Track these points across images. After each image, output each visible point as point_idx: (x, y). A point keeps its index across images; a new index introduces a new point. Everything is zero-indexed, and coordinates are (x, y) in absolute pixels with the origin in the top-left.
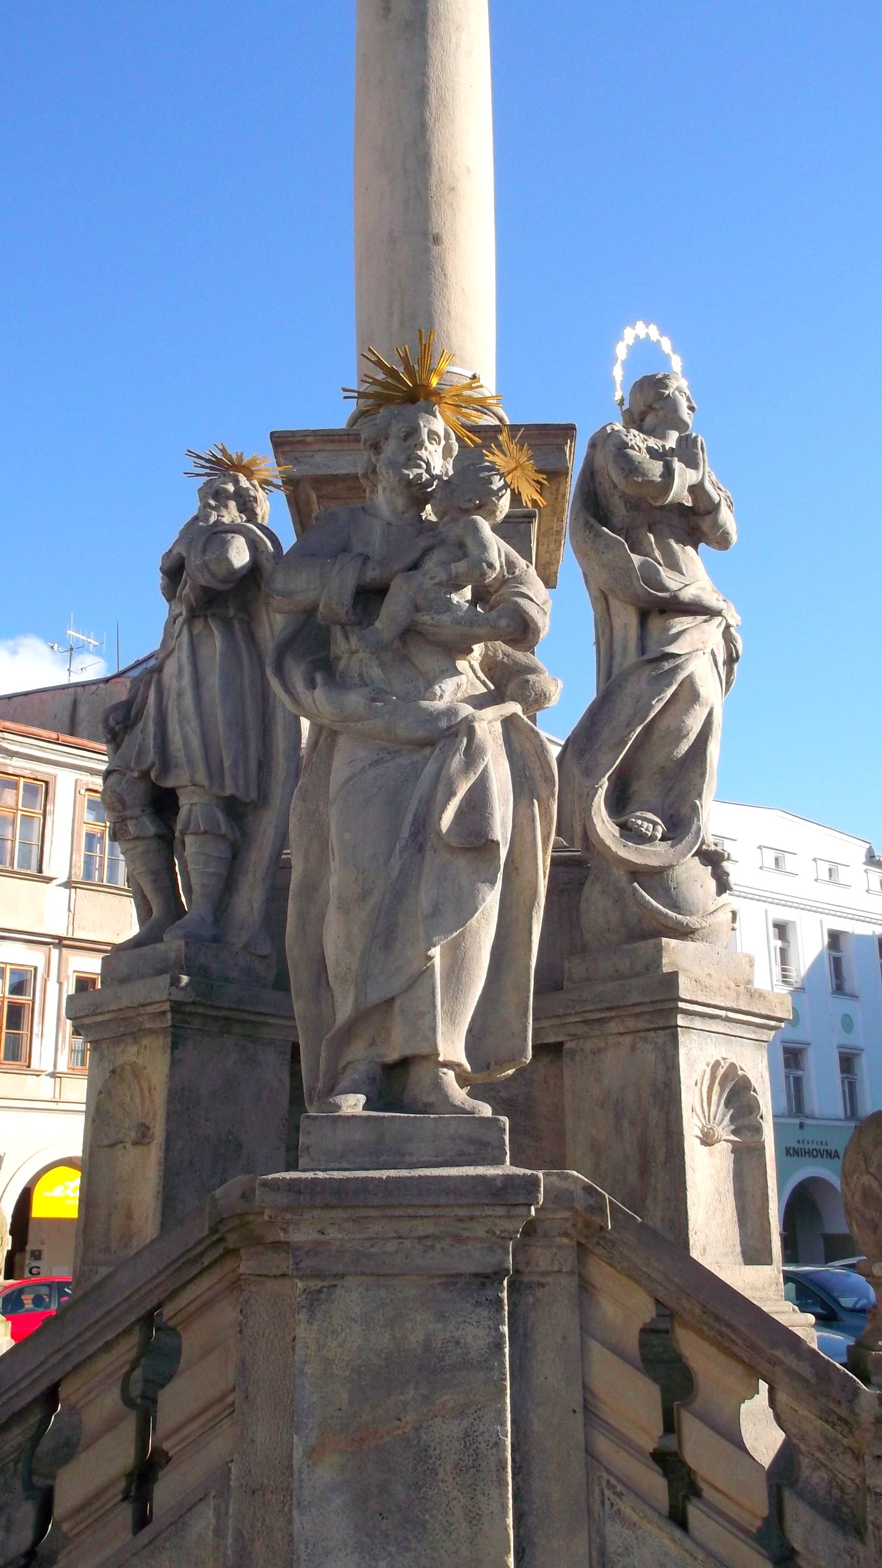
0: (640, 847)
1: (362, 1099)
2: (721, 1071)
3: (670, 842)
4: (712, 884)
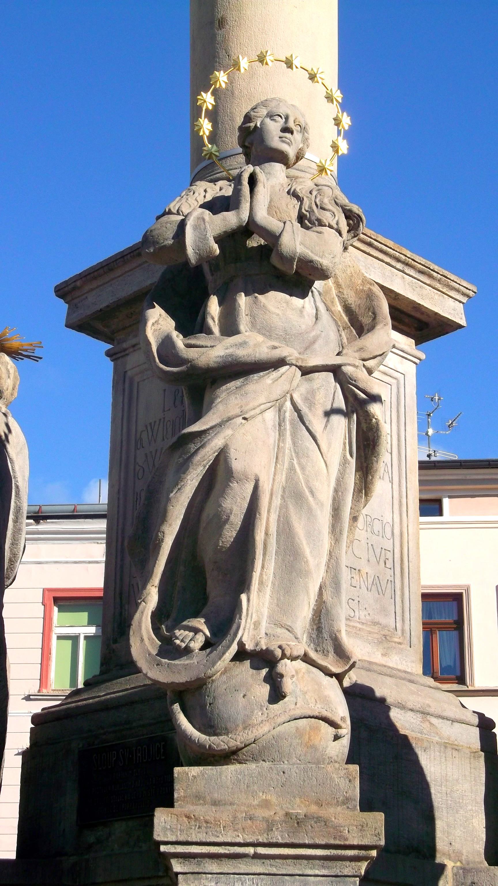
0: (177, 662)
3: (208, 650)
4: (266, 689)
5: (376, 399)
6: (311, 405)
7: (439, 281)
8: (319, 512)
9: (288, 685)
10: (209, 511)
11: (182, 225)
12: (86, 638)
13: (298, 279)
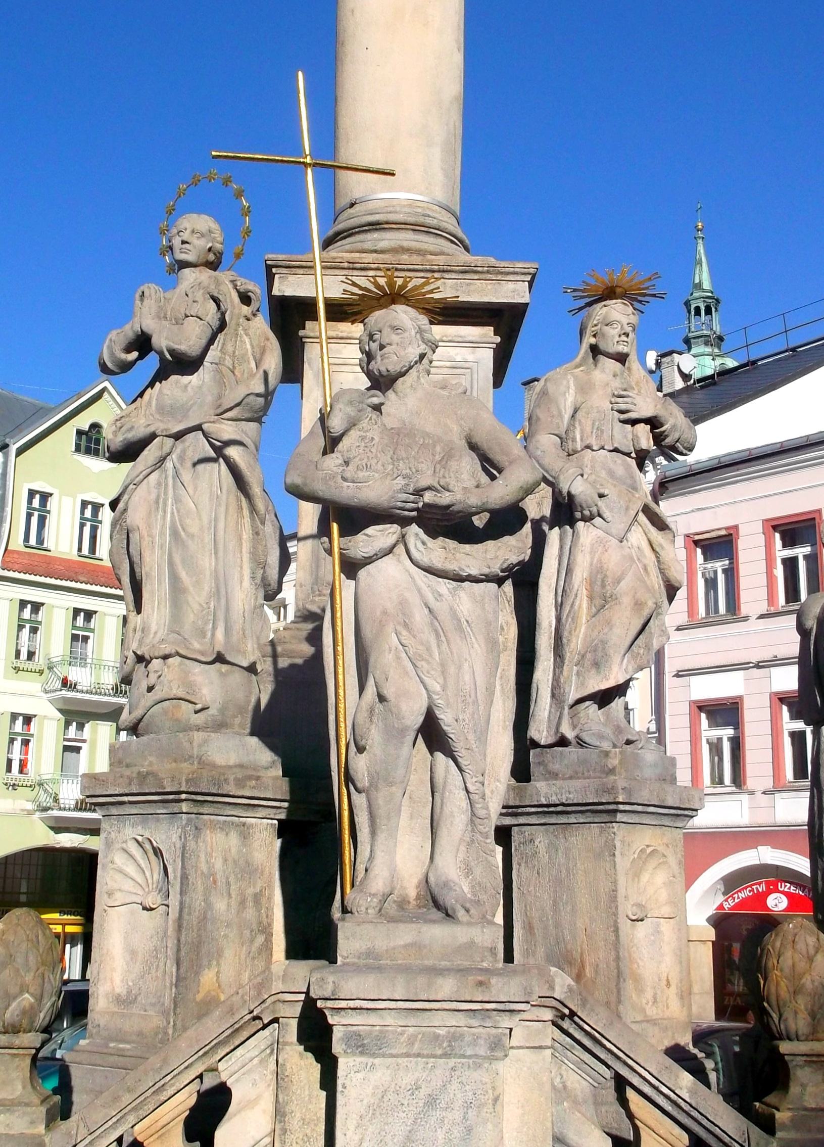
7: (488, 272)
8: (190, 542)
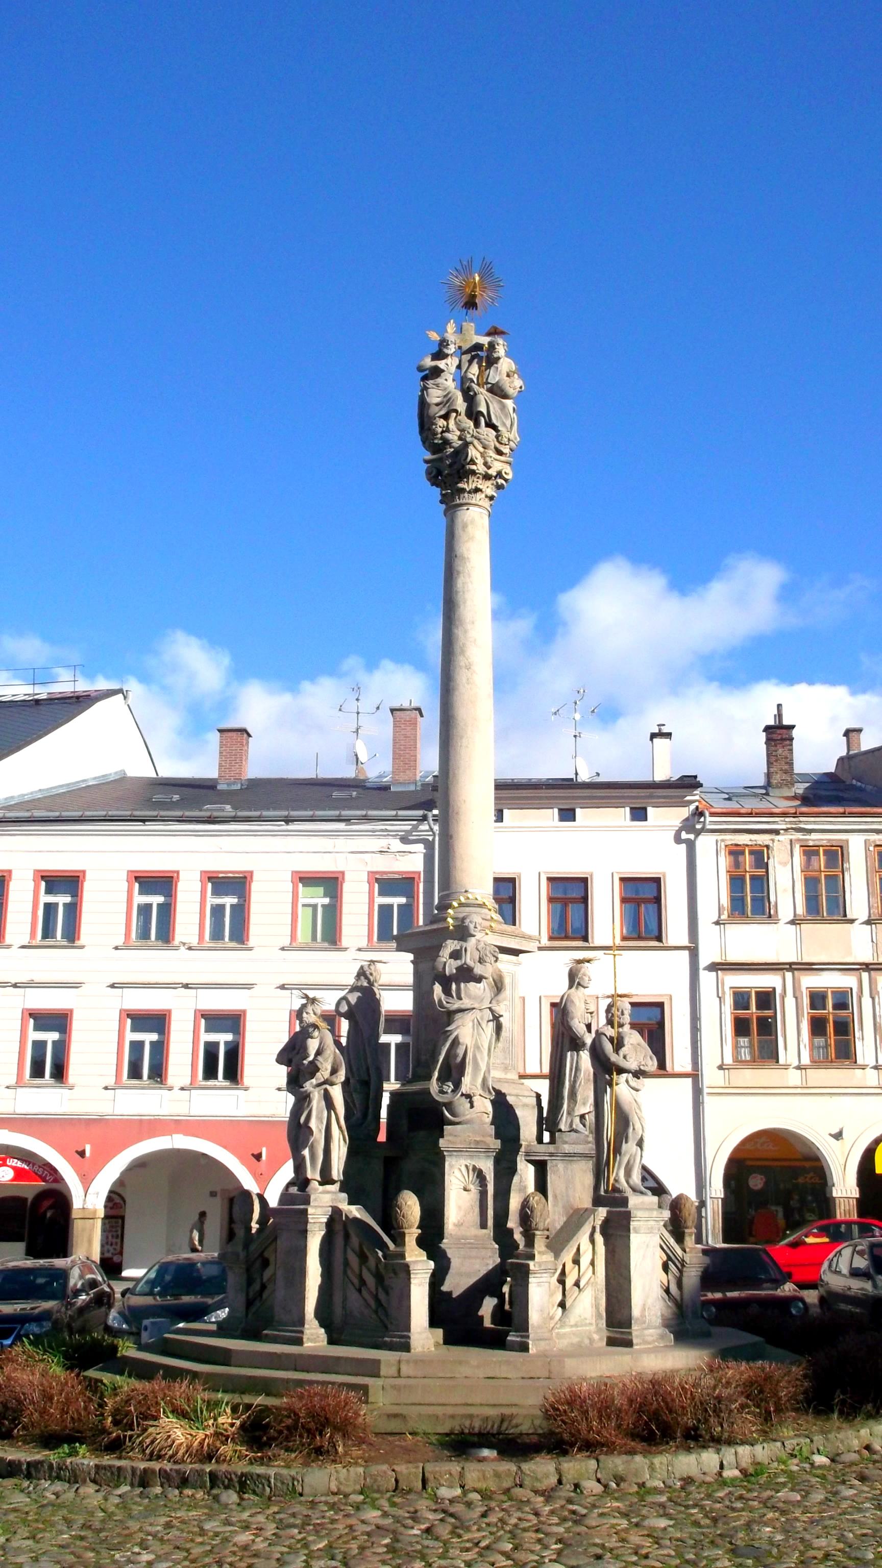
1: (296, 1188)
2: (471, 1168)
4: (469, 1105)
5: (501, 1016)
6: (482, 1019)
9: (475, 1104)
10: (453, 1052)
11: (445, 963)
12: (323, 906)
13: (479, 979)
